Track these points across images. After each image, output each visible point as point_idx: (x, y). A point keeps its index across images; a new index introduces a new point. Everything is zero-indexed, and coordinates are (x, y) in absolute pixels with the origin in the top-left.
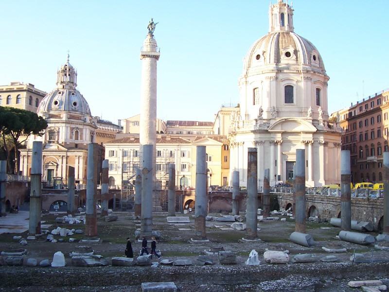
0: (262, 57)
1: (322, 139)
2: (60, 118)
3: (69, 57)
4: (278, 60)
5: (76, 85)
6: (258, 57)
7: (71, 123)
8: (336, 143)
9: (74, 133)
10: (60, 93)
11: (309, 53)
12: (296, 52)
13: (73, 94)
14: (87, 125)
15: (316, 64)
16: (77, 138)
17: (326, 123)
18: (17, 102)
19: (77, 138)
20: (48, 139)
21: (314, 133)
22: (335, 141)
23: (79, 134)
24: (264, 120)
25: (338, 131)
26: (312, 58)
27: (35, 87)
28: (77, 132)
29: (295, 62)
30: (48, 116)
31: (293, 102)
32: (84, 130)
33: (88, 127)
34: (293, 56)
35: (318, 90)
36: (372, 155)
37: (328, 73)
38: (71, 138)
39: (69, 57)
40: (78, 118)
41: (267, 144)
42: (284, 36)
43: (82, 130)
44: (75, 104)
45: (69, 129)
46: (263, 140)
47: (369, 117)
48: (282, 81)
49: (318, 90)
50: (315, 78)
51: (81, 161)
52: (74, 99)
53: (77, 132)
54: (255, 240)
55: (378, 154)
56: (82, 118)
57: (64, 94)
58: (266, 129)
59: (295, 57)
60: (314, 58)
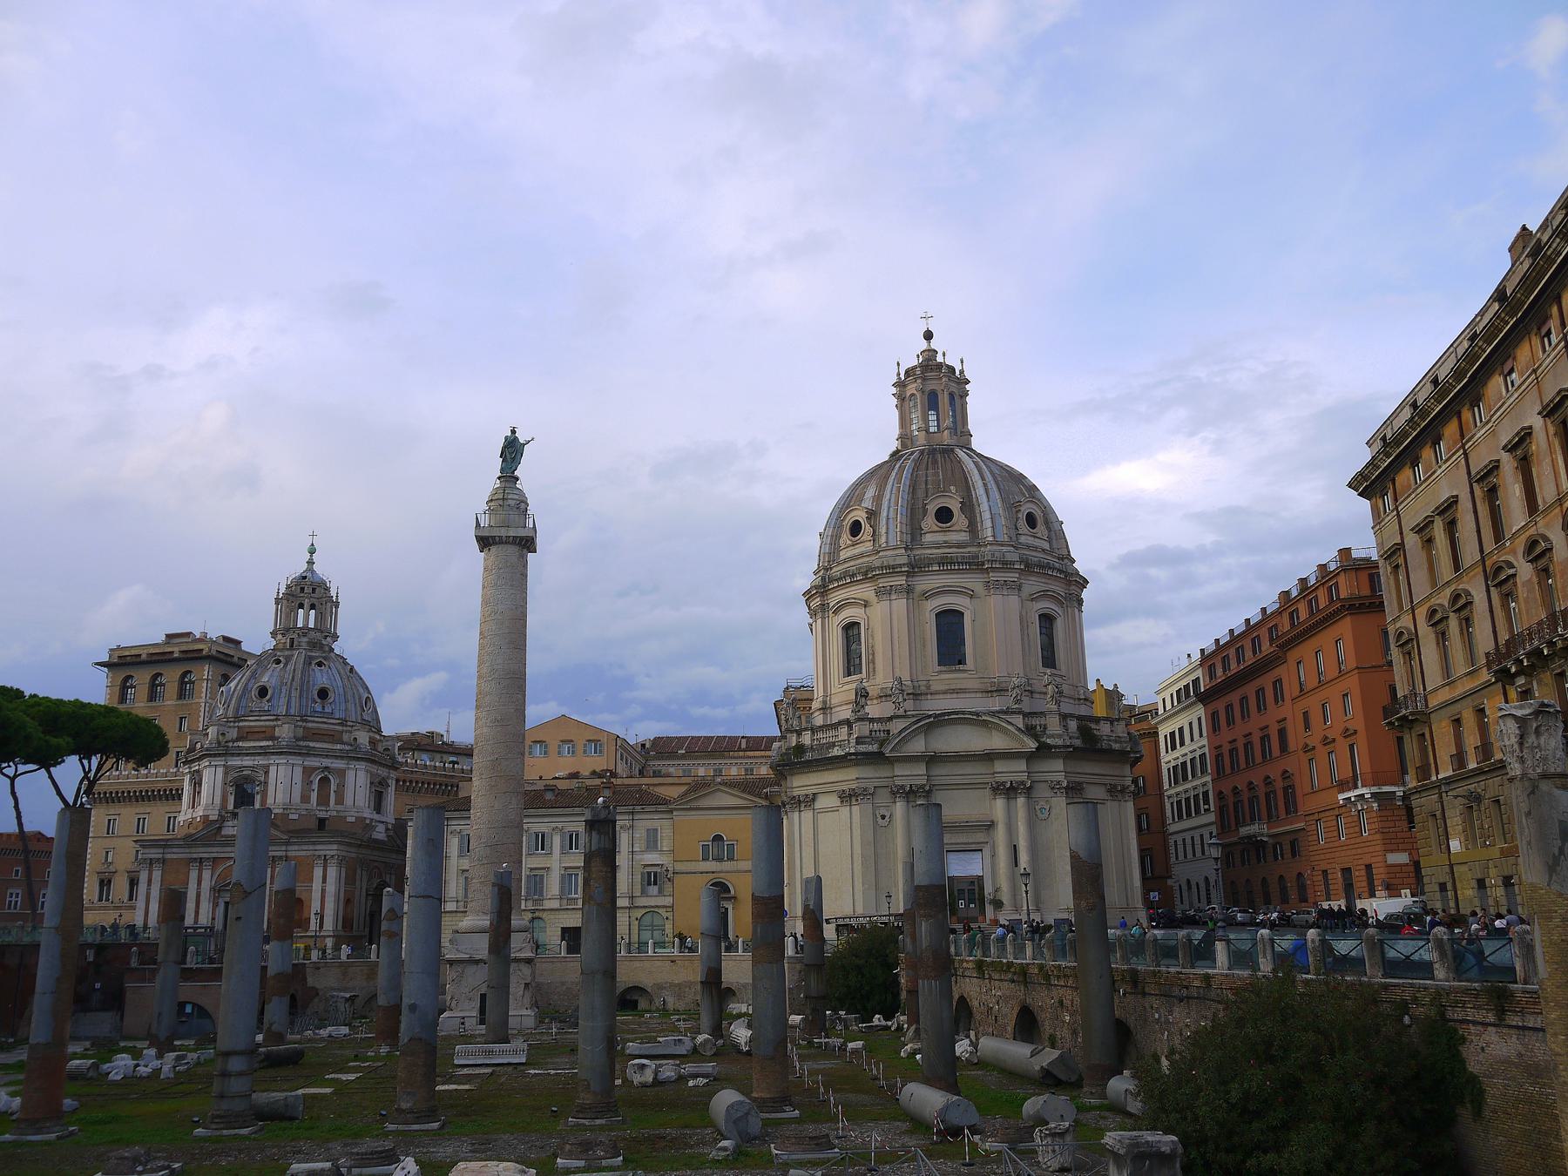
0: (866, 529)
1: (1055, 769)
2: (273, 738)
3: (312, 551)
4: (914, 532)
5: (335, 637)
6: (856, 528)
7: (308, 755)
8: (1115, 786)
9: (315, 786)
10: (278, 662)
11: (1012, 507)
12: (969, 506)
13: (320, 664)
14: (358, 759)
15: (1034, 540)
16: (323, 800)
17: (1073, 725)
18: (152, 696)
19: (323, 800)
20: (231, 807)
21: (1030, 757)
22: (1107, 780)
23: (333, 787)
24: (872, 720)
25: (1116, 746)
26: (1022, 523)
27: (244, 647)
28: (324, 781)
29: (963, 537)
30: (300, 732)
31: (962, 661)
32: (350, 775)
33: (362, 765)
34: (960, 520)
35: (1047, 620)
36: (1253, 820)
37: (1081, 566)
38: (305, 798)
39: (312, 551)
40: (333, 737)
41: (883, 797)
42: (935, 462)
43: (341, 773)
44: (323, 694)
45: (298, 771)
46: (870, 785)
47: (1234, 698)
48: (926, 596)
49: (1047, 620)
50: (1033, 585)
51: (332, 872)
52: (321, 678)
53: (324, 781)
54: (598, 1122)
55: (1270, 816)
56: (346, 737)
57: (290, 667)
58: (874, 748)
59: (966, 522)
60: (1031, 521)
